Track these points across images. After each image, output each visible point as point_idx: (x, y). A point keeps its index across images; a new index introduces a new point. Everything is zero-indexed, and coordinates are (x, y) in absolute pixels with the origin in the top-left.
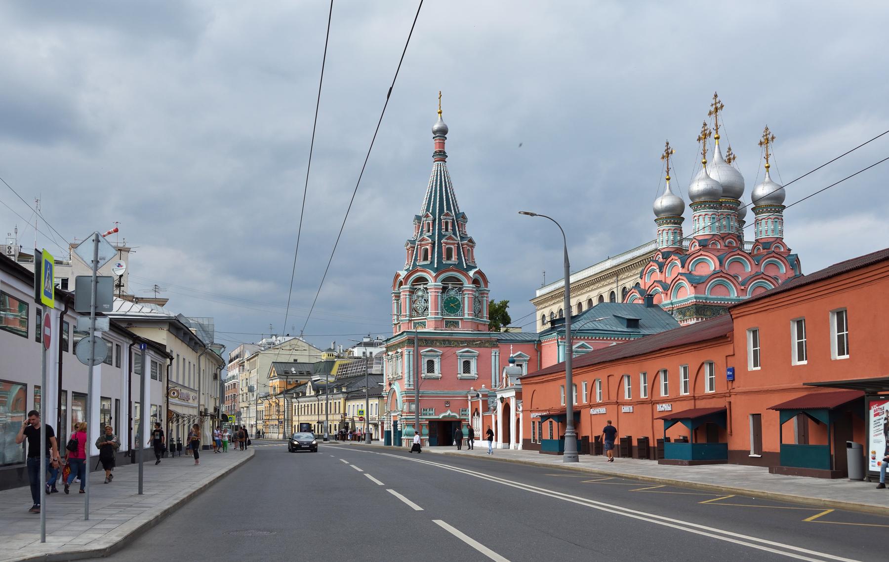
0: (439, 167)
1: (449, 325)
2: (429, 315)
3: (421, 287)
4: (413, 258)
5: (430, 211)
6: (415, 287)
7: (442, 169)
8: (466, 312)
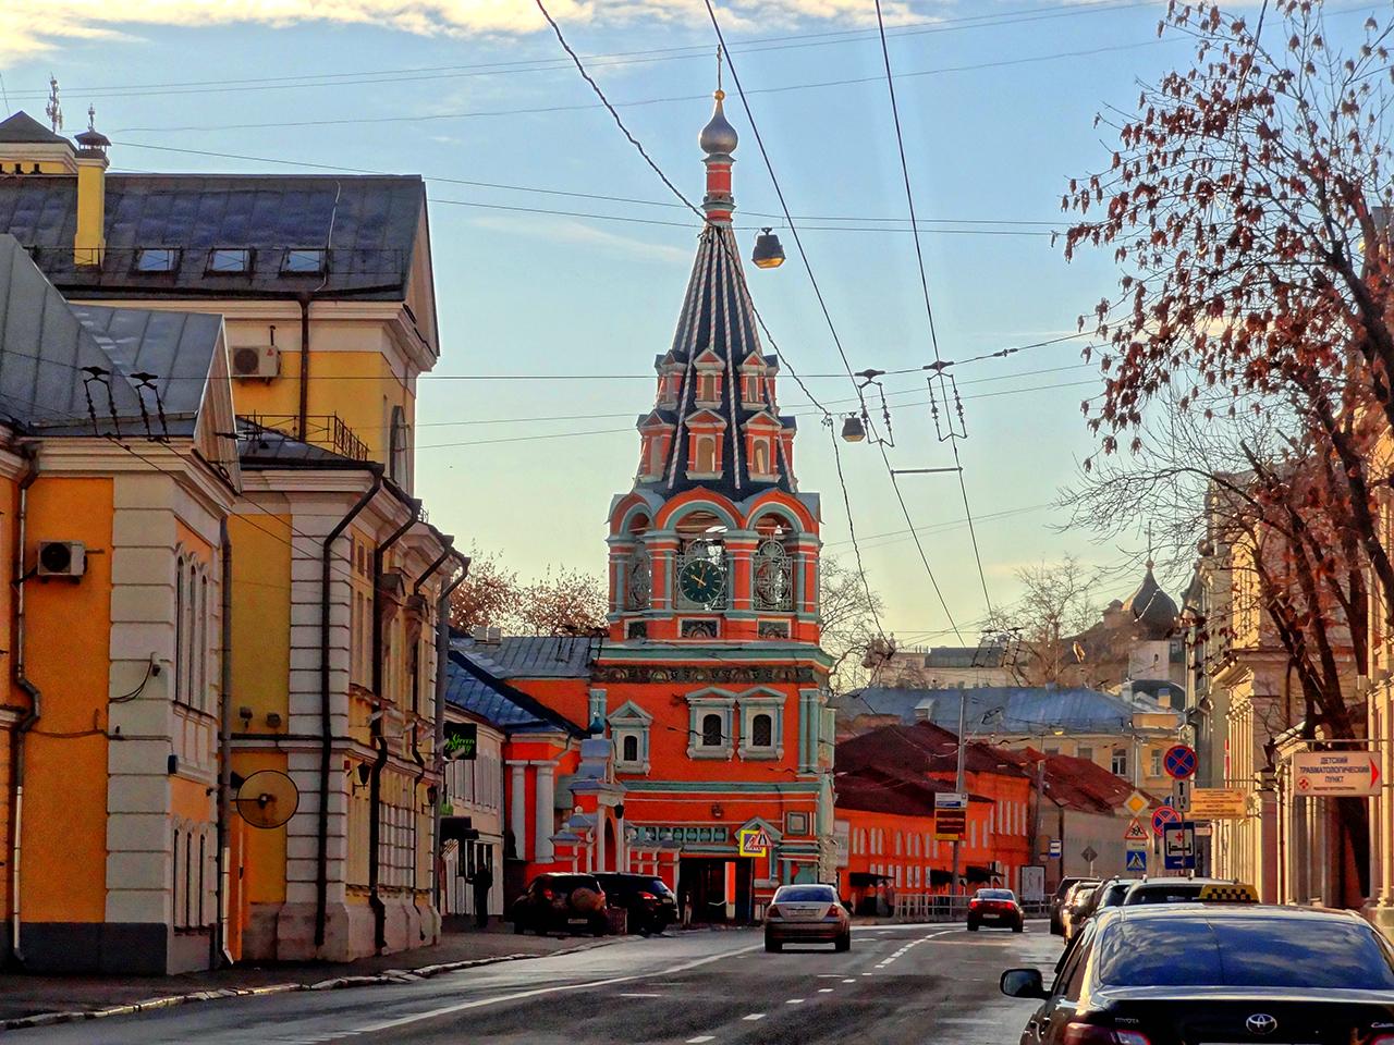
8: (801, 602)
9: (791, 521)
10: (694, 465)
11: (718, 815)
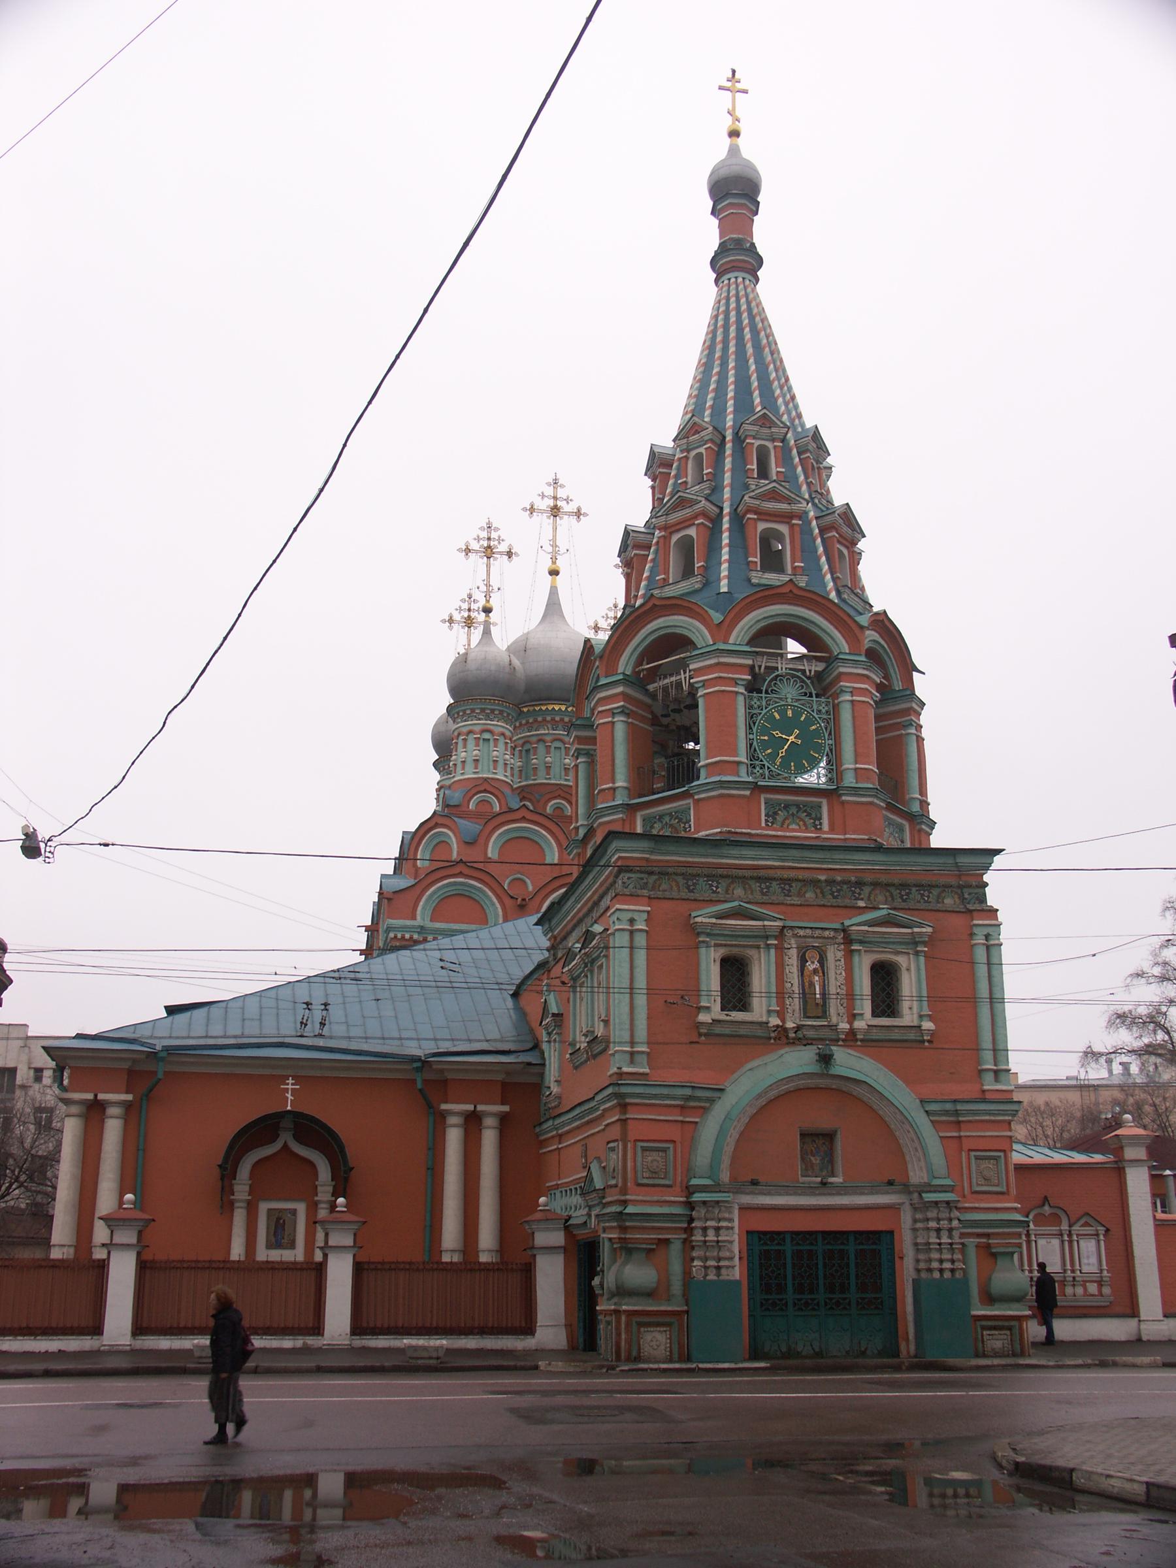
0: (733, 287)
1: (779, 819)
2: (703, 773)
7: (742, 293)
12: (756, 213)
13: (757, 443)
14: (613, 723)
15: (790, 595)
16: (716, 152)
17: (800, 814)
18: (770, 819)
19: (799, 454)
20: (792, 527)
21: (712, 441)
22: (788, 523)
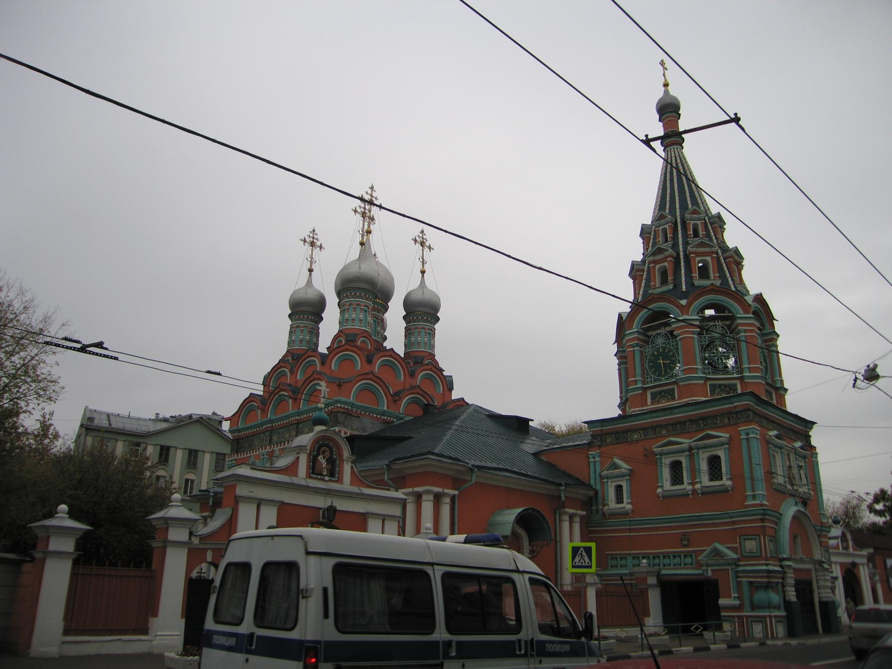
0: (673, 152)
1: (716, 392)
3: (662, 331)
4: (643, 285)
5: (667, 211)
6: (650, 333)
7: (677, 155)
9: (730, 307)
10: (655, 285)
11: (685, 543)
12: (679, 119)
13: (692, 222)
14: (634, 351)
15: (713, 290)
16: (660, 93)
17: (726, 389)
18: (712, 393)
19: (711, 224)
20: (712, 258)
21: (671, 222)
22: (710, 256)
